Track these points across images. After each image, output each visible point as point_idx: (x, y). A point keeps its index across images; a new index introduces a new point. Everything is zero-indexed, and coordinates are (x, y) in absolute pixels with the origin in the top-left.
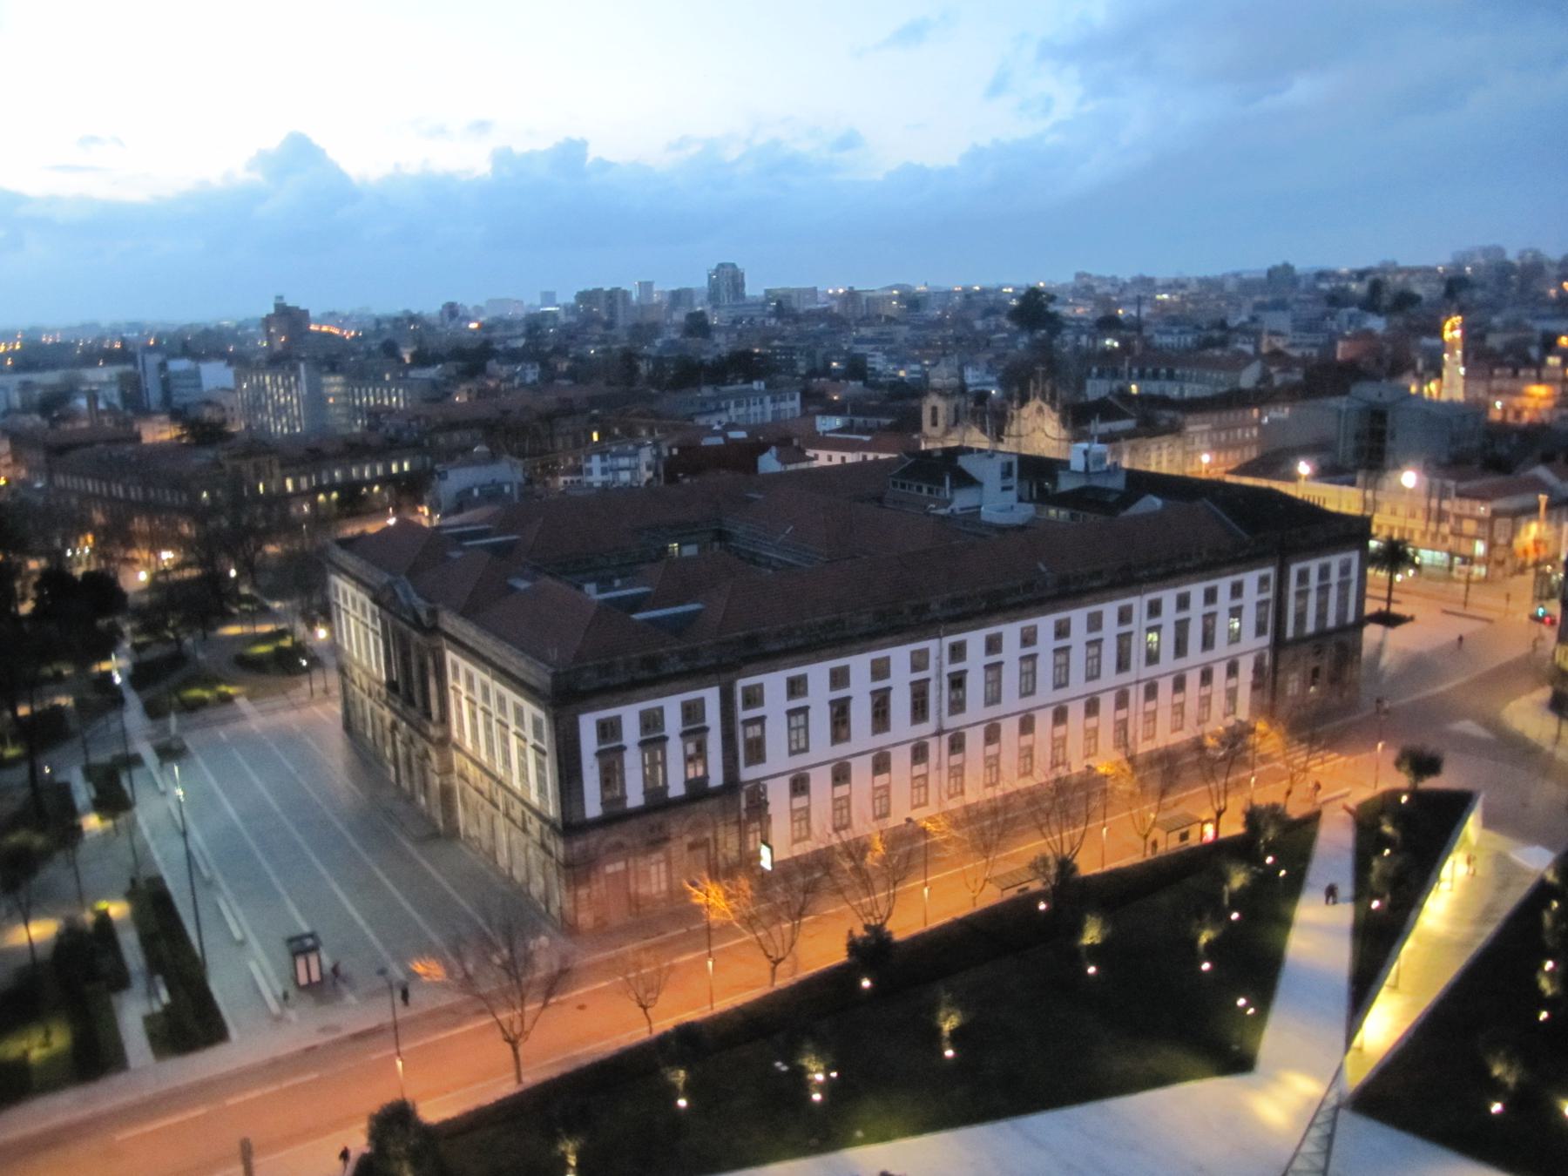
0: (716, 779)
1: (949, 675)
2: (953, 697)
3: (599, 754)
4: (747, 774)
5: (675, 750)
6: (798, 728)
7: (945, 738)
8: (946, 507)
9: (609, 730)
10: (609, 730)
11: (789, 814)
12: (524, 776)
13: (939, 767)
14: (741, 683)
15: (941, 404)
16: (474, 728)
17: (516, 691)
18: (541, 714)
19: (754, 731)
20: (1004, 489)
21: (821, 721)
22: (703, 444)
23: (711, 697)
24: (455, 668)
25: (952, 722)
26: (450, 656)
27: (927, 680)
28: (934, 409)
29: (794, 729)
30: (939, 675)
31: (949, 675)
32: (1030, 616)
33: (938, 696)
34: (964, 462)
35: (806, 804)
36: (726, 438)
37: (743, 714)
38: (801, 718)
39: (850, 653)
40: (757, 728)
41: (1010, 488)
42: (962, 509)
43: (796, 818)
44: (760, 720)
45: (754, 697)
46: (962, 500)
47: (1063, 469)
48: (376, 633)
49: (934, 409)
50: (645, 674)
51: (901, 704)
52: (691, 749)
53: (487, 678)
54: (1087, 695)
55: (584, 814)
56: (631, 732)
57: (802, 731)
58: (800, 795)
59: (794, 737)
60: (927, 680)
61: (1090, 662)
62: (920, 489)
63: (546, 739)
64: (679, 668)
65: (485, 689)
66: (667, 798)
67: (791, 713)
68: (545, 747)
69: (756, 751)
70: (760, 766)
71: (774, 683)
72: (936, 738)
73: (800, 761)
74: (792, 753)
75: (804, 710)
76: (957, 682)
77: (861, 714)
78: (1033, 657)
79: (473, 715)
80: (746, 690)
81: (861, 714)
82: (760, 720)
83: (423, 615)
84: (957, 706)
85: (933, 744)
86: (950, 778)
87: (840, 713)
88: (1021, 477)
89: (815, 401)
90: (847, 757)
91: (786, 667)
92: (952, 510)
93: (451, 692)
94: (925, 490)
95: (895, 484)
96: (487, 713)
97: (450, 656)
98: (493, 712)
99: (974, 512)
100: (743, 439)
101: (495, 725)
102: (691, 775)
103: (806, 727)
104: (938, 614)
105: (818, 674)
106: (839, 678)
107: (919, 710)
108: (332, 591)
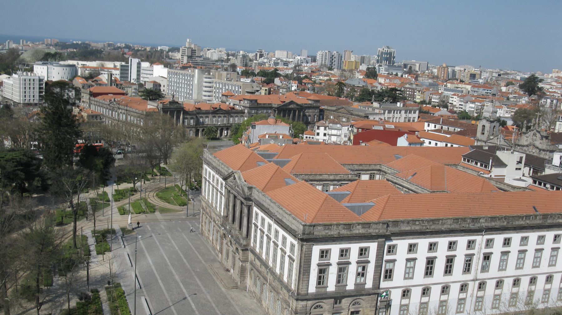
0: (369, 284)
1: (484, 254)
2: (484, 264)
3: (319, 265)
4: (384, 284)
5: (353, 269)
6: (410, 268)
7: (477, 283)
8: (488, 174)
9: (324, 254)
10: (324, 254)
11: (399, 306)
12: (282, 268)
13: (472, 296)
14: (388, 243)
15: (487, 125)
16: (262, 242)
17: (284, 230)
18: (295, 242)
19: (389, 266)
20: (517, 169)
21: (421, 266)
22: (373, 128)
23: (373, 246)
24: (257, 214)
25: (481, 276)
26: (255, 209)
27: (474, 255)
28: (484, 126)
29: (408, 268)
30: (479, 253)
31: (484, 254)
32: (526, 232)
33: (477, 263)
34: (499, 154)
35: (407, 303)
36: (384, 127)
37: (386, 257)
38: (412, 263)
39: (440, 237)
40: (392, 264)
41: (520, 169)
42: (495, 176)
43: (402, 309)
44: (394, 261)
45: (392, 250)
46: (496, 172)
47: (548, 163)
48: (221, 194)
49: (484, 126)
50: (344, 232)
51: (459, 264)
52: (360, 270)
53: (272, 223)
54: (547, 273)
55: (308, 291)
56: (334, 258)
57: (411, 270)
58: (406, 298)
59: (407, 271)
60: (474, 255)
61: (552, 258)
62: (476, 163)
63: (296, 254)
64: (360, 231)
65: (270, 226)
66: (345, 290)
67: (408, 260)
68: (295, 258)
69: (389, 275)
70: (389, 282)
71: (402, 244)
72: (473, 282)
73: (409, 283)
74: (405, 278)
75: (414, 260)
76: (487, 257)
77: (440, 266)
78: (541, 250)
79: (262, 237)
80: (389, 247)
81: (440, 266)
82: (394, 261)
83: (246, 190)
84: (485, 269)
85: (471, 284)
86: (476, 302)
87: (430, 262)
88: (526, 165)
89: (425, 115)
90: (430, 284)
91: (409, 239)
92: (491, 176)
93: (253, 226)
94: (479, 164)
95: (464, 159)
96: (269, 238)
97: (255, 209)
98: (272, 238)
99: (500, 180)
100: (392, 129)
101: (272, 244)
102: (358, 281)
103: (414, 268)
104: (483, 224)
105: (423, 243)
106: (432, 247)
107: (467, 268)
108: (204, 171)
